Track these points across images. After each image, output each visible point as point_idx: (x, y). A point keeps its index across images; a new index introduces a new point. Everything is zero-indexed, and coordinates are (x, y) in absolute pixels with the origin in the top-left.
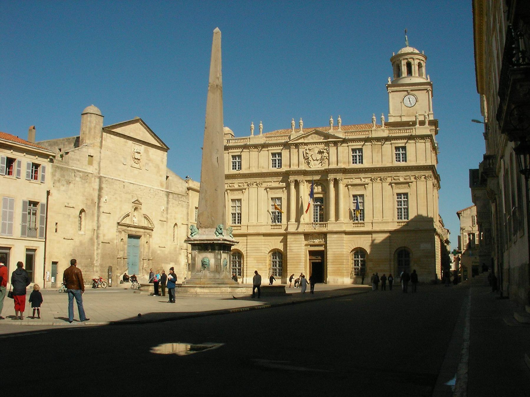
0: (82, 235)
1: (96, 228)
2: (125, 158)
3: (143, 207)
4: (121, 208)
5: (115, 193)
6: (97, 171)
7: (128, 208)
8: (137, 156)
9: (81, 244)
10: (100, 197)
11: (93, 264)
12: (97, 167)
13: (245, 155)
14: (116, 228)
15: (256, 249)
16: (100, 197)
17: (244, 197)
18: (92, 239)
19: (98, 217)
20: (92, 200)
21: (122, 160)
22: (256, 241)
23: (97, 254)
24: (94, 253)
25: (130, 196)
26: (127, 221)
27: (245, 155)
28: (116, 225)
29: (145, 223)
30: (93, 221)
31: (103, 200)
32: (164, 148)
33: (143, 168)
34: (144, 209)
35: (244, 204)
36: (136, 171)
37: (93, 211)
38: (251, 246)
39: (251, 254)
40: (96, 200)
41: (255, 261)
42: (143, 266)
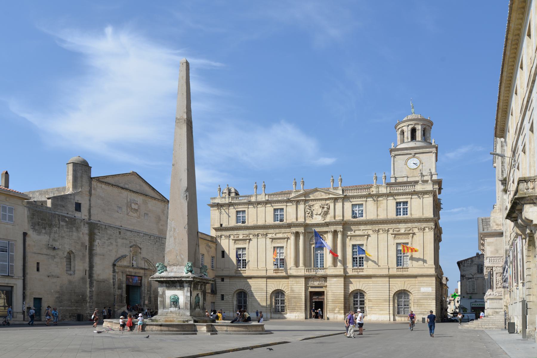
0: (71, 275)
1: (88, 269)
5: (109, 239)
9: (70, 282)
10: (92, 240)
14: (112, 269)
16: (92, 240)
18: (83, 279)
23: (90, 291)
26: (125, 263)
34: (144, 254)
37: (83, 254)
40: (87, 244)
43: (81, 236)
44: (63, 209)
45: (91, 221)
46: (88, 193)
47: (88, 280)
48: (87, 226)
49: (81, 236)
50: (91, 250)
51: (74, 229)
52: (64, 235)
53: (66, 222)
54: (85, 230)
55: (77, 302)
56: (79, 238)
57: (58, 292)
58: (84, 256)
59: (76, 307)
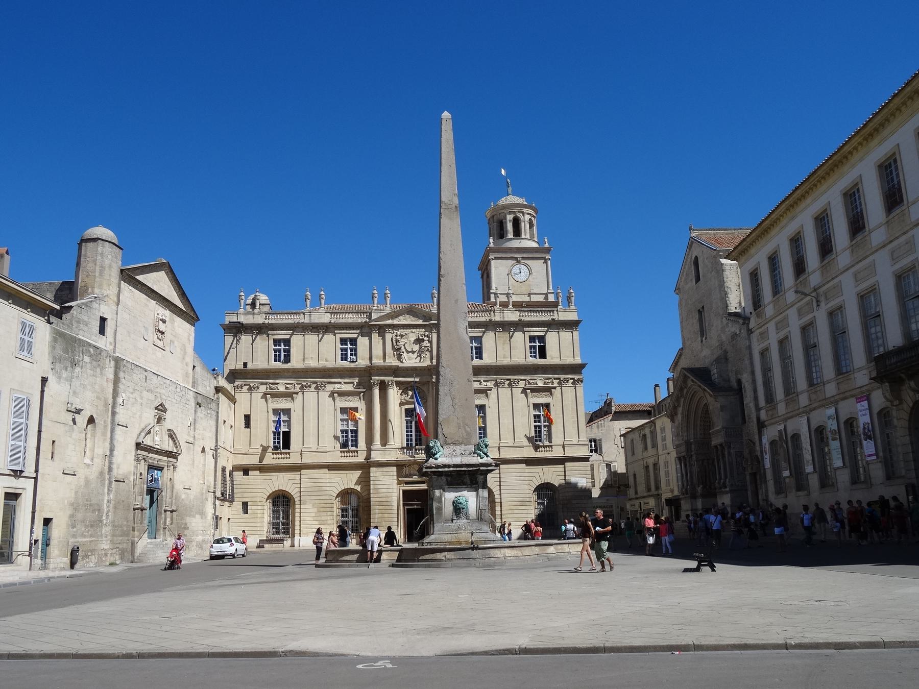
1: (108, 453)
2: (146, 329)
3: (168, 415)
4: (140, 417)
6: (112, 347)
7: (149, 416)
8: (162, 327)
9: (87, 482)
10: (115, 394)
11: (101, 521)
12: (112, 340)
13: (297, 340)
14: (133, 453)
15: (316, 489)
16: (115, 394)
17: (295, 406)
18: (101, 473)
19: (112, 431)
20: (106, 400)
21: (142, 330)
22: (317, 476)
23: (108, 501)
24: (103, 500)
25: (152, 397)
26: (148, 441)
27: (297, 340)
28: (134, 448)
29: (168, 446)
30: (105, 440)
31: (120, 400)
32: (191, 316)
33: (167, 349)
34: (170, 422)
35: (293, 415)
36: (159, 353)
37: (105, 422)
38: (308, 485)
39: (308, 498)
40: (110, 401)
41: (316, 510)
42: (165, 522)
43: (105, 384)
44: (86, 328)
45: (117, 354)
46: (115, 299)
47: (107, 477)
48: (113, 363)
49: (105, 384)
50: (114, 413)
51: (98, 370)
52: (86, 382)
53: (91, 356)
54: (110, 373)
55: (92, 526)
56: (103, 390)
57: (72, 504)
58: (105, 426)
59: (91, 536)
